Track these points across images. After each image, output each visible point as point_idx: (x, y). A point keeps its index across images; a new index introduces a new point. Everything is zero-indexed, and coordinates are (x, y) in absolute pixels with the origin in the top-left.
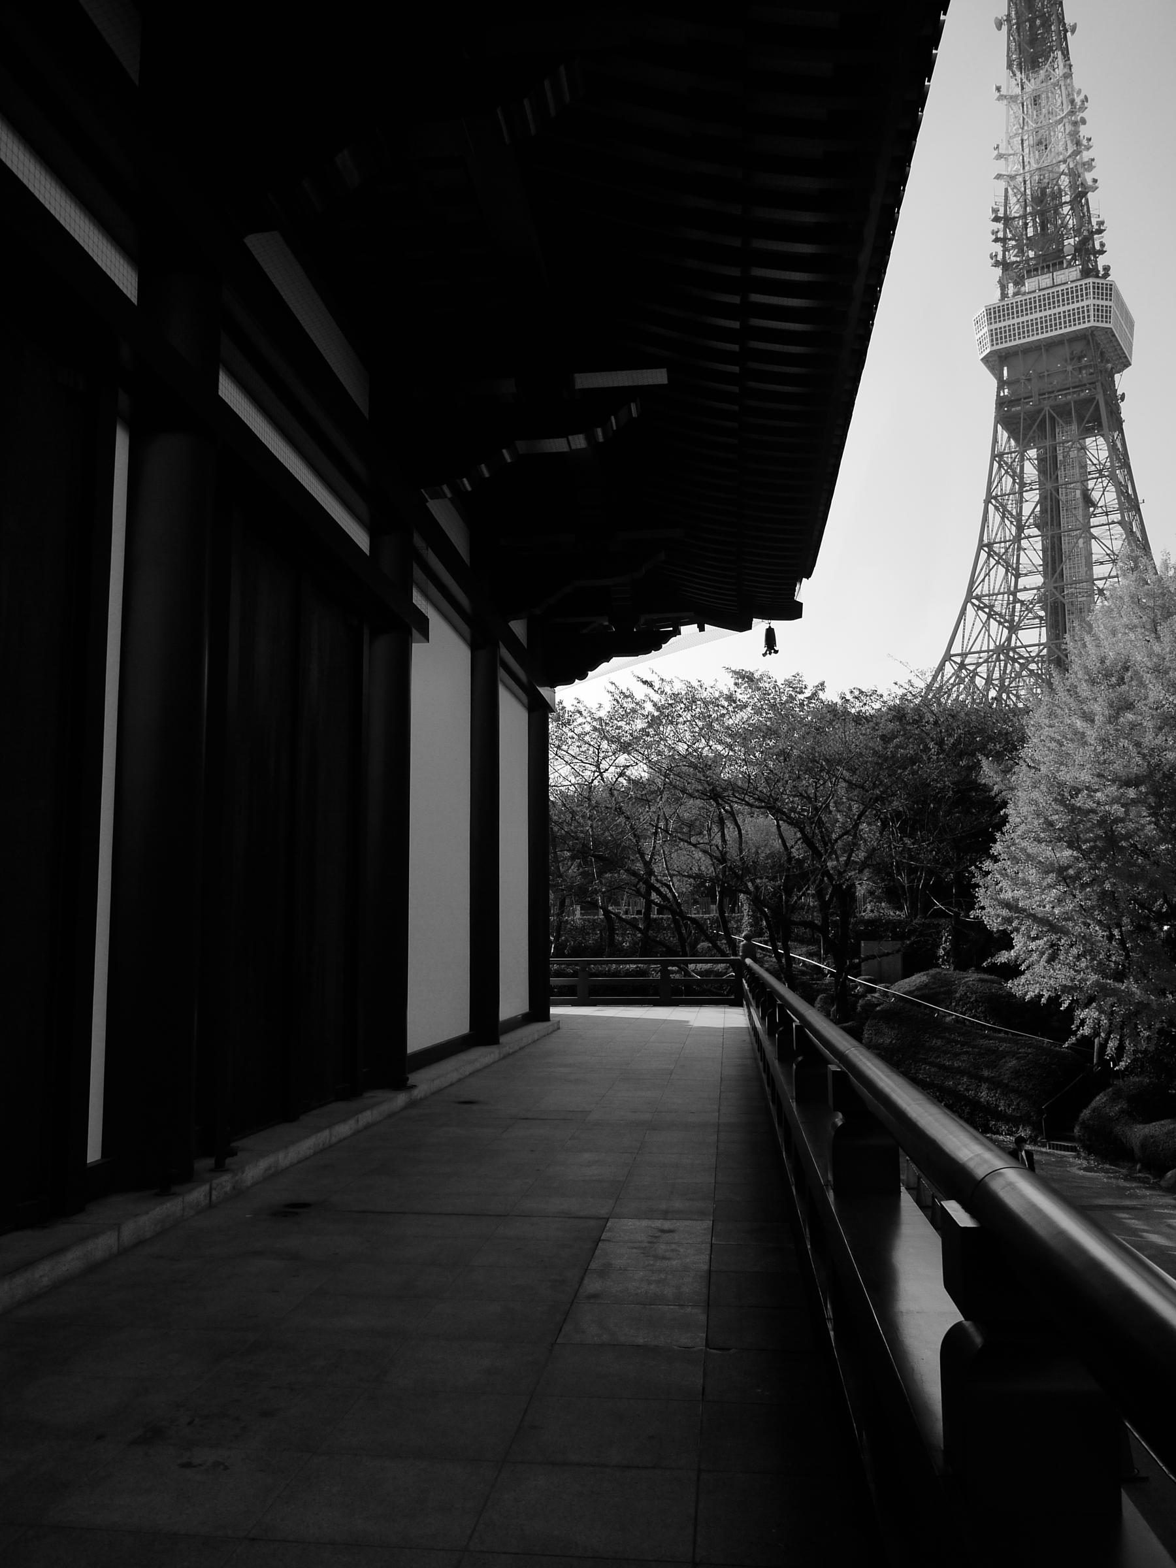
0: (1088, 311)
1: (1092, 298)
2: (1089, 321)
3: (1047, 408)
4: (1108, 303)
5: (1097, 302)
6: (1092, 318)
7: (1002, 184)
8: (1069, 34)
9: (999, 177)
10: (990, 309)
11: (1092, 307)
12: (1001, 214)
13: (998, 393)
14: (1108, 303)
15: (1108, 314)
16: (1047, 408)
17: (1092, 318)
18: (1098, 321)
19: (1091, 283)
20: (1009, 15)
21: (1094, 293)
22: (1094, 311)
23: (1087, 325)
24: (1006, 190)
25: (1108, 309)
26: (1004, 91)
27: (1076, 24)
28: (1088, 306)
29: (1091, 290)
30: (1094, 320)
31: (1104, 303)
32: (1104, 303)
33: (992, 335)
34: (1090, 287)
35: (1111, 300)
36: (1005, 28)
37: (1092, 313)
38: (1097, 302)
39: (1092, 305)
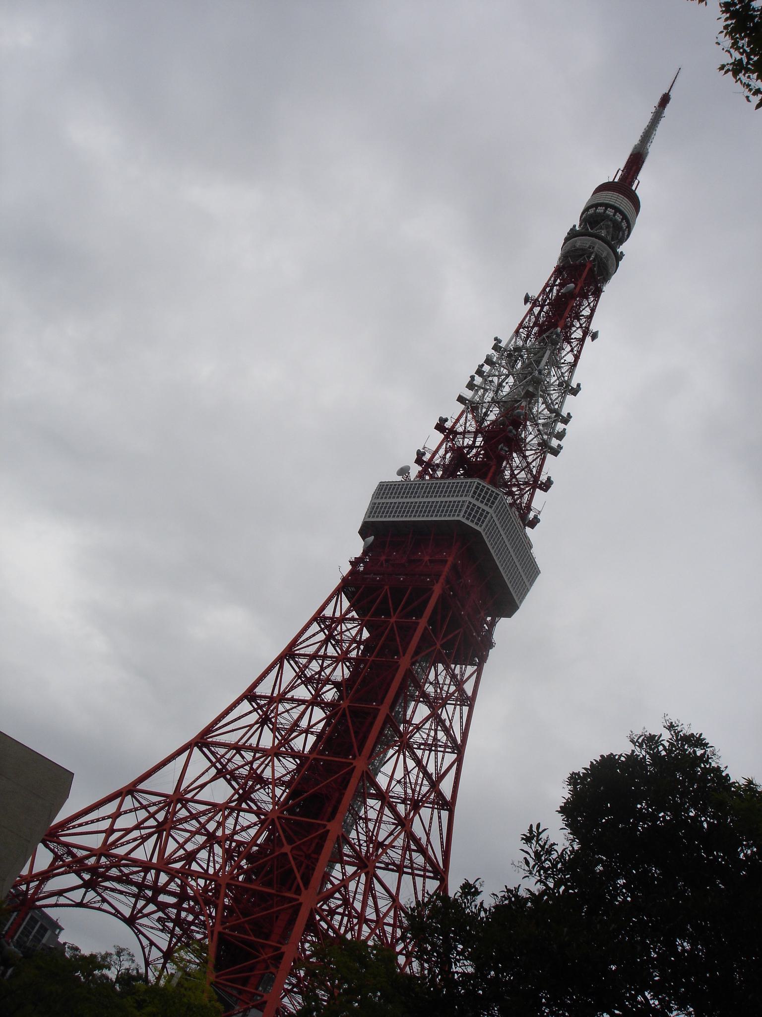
0: (462, 506)
1: (470, 496)
4: (487, 509)
5: (474, 501)
8: (588, 339)
9: (461, 399)
11: (467, 503)
12: (448, 425)
14: (487, 509)
17: (462, 513)
18: (468, 519)
19: (476, 483)
21: (475, 493)
23: (456, 518)
25: (484, 514)
26: (503, 345)
27: (597, 332)
32: (483, 506)
34: (473, 485)
35: (491, 507)
37: (464, 509)
38: (474, 501)
39: (468, 502)
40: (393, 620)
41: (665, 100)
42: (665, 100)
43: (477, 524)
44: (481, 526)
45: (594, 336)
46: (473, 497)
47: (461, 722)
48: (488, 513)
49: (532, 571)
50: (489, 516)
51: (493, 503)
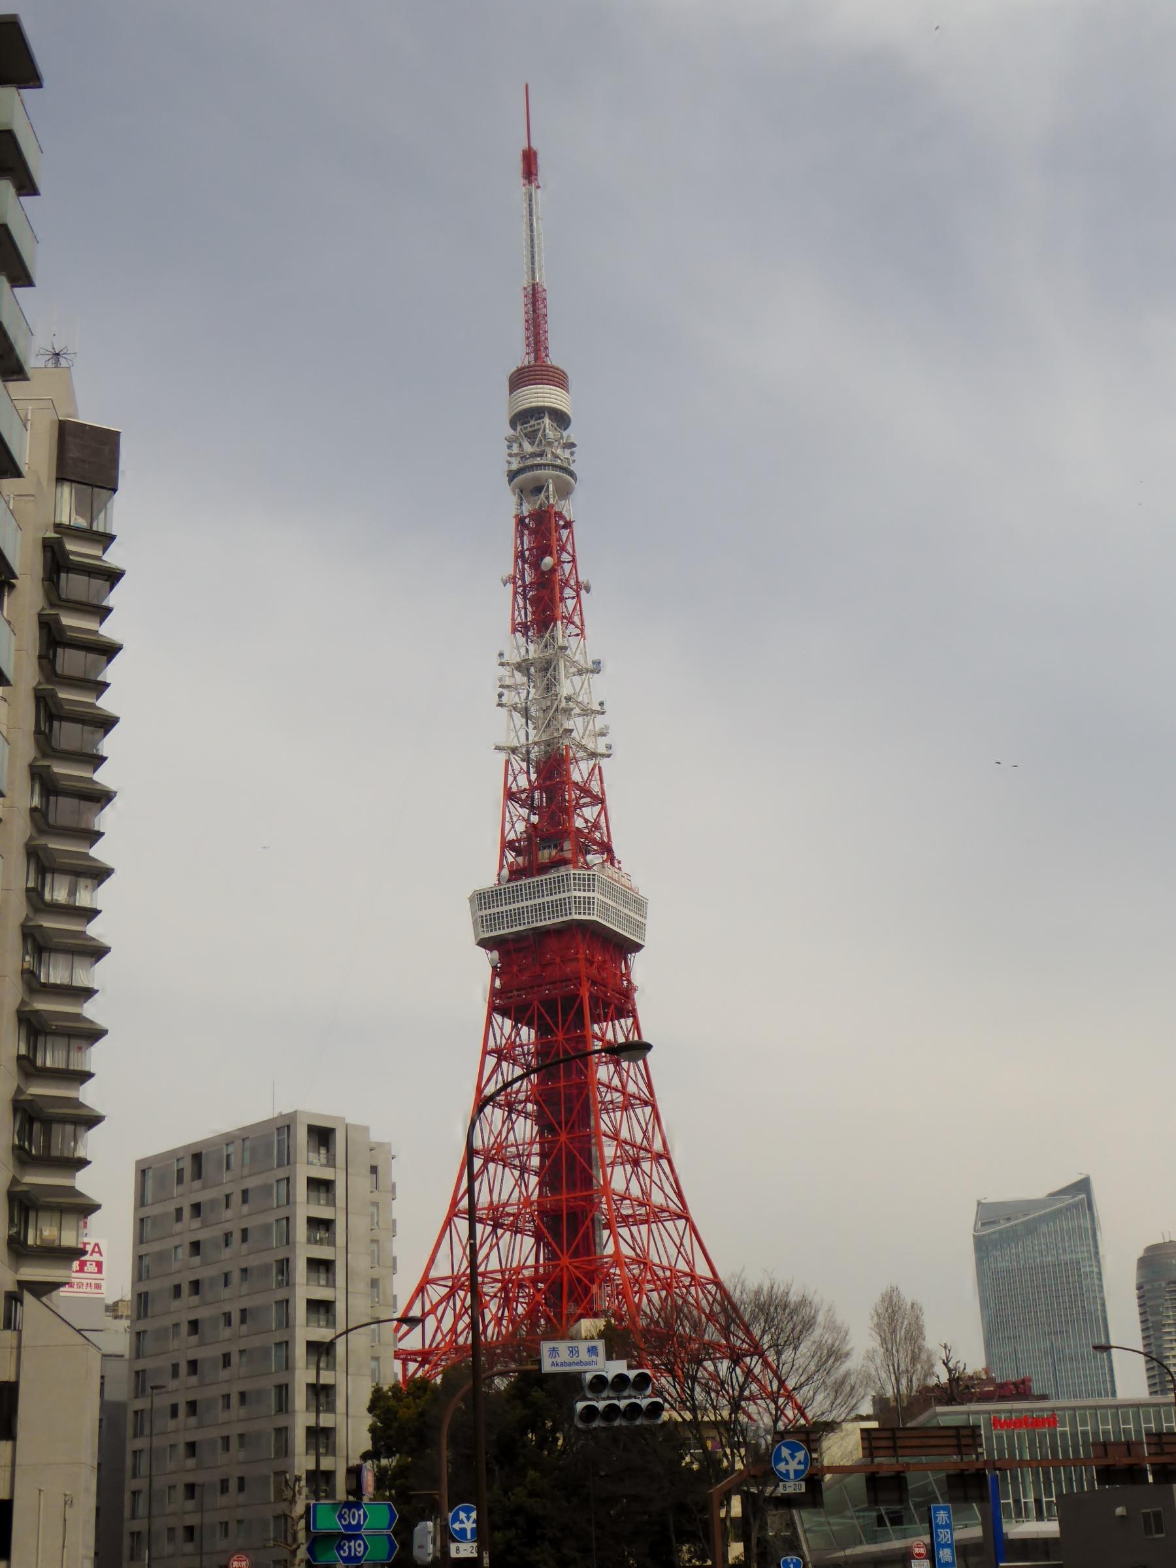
2: (570, 914)
3: (536, 1002)
4: (591, 894)
5: (577, 894)
6: (573, 911)
7: (502, 756)
8: (583, 593)
10: (480, 894)
13: (493, 981)
14: (591, 894)
15: (592, 906)
16: (536, 1002)
20: (514, 577)
22: (575, 903)
23: (569, 918)
24: (507, 762)
25: (590, 902)
28: (569, 898)
29: (572, 882)
30: (576, 913)
31: (587, 894)
32: (587, 894)
33: (482, 923)
35: (594, 891)
36: (510, 586)
40: (560, 1037)
41: (529, 160)
42: (529, 160)
43: (589, 914)
44: (593, 914)
45: (588, 590)
46: (575, 890)
47: (644, 1080)
48: (593, 898)
49: (640, 905)
50: (596, 901)
51: (594, 885)
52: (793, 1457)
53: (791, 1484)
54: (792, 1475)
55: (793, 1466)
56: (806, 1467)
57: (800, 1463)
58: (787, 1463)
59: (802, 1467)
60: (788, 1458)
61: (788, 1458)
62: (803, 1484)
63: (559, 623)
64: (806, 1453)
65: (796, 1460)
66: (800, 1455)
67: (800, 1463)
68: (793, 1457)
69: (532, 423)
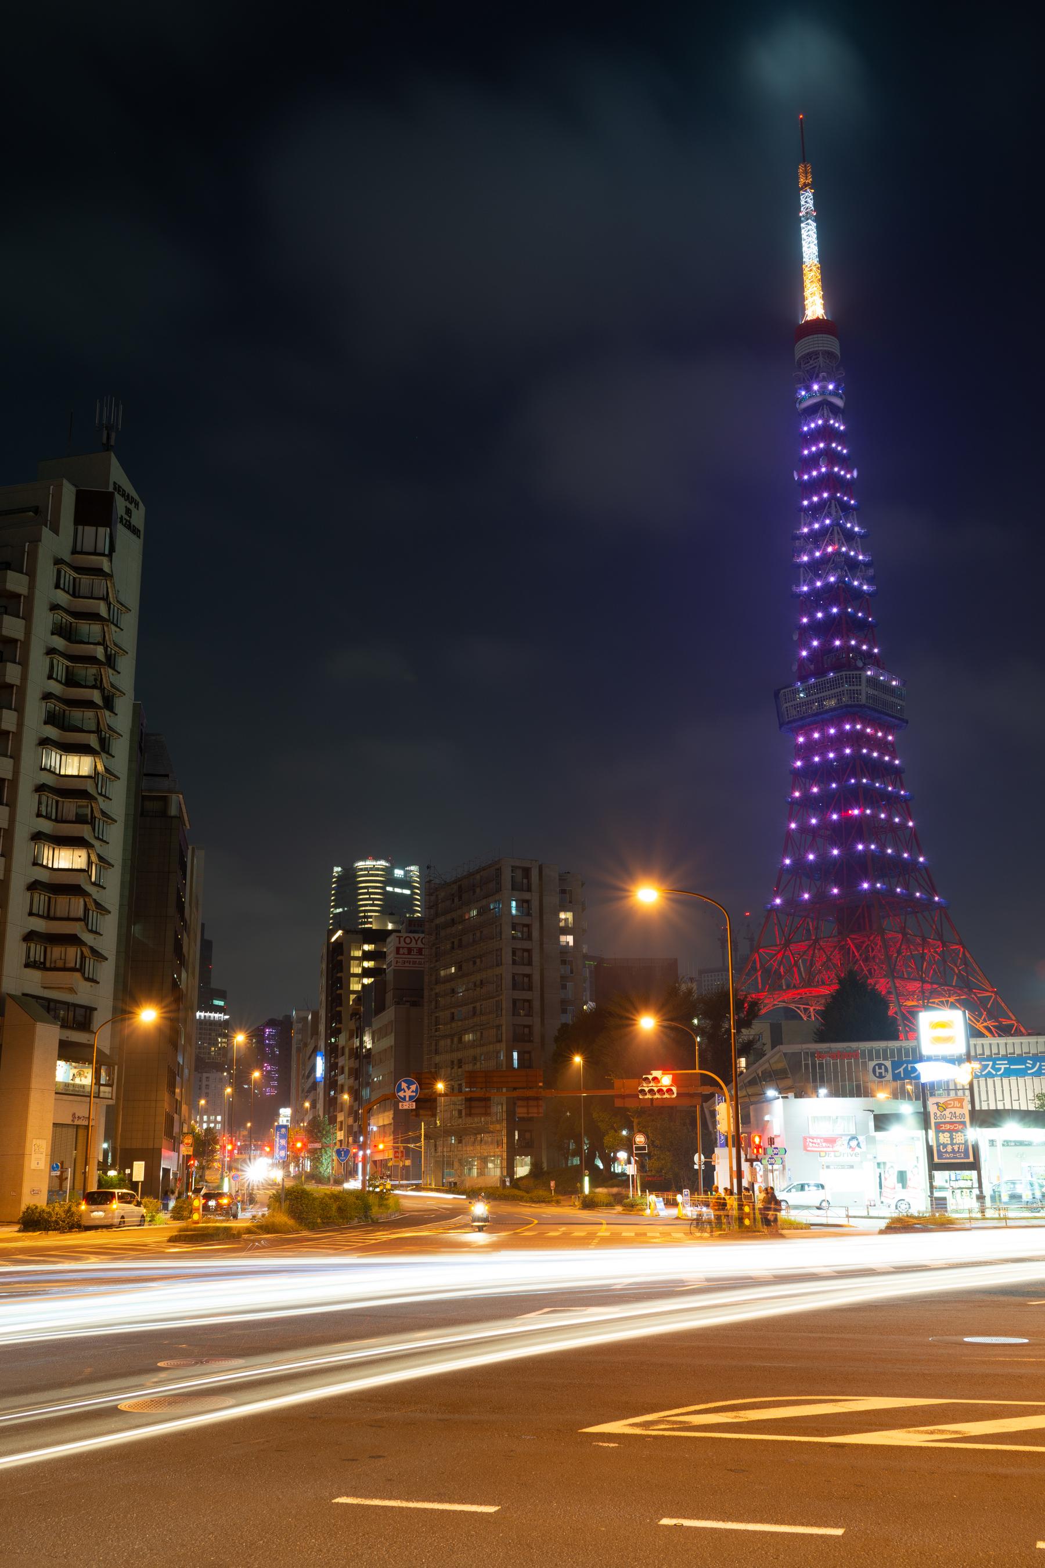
31: (855, 688)
52: (409, 1088)
53: (407, 1104)
54: (407, 1099)
55: (408, 1093)
56: (416, 1094)
57: (413, 1092)
58: (405, 1092)
59: (414, 1094)
60: (406, 1089)
61: (406, 1089)
62: (414, 1103)
63: (833, 501)
64: (417, 1086)
65: (411, 1090)
66: (413, 1087)
67: (413, 1092)
68: (409, 1088)
69: (811, 362)
